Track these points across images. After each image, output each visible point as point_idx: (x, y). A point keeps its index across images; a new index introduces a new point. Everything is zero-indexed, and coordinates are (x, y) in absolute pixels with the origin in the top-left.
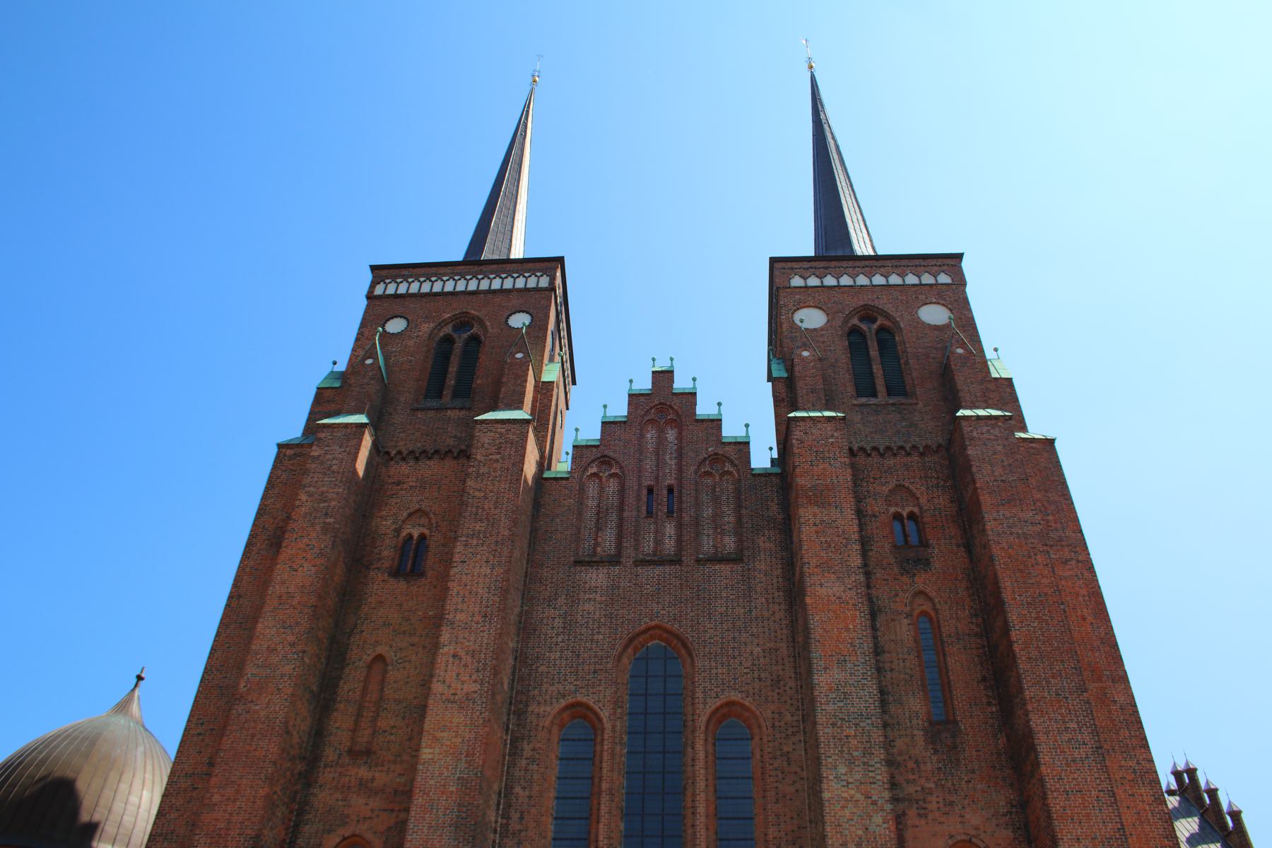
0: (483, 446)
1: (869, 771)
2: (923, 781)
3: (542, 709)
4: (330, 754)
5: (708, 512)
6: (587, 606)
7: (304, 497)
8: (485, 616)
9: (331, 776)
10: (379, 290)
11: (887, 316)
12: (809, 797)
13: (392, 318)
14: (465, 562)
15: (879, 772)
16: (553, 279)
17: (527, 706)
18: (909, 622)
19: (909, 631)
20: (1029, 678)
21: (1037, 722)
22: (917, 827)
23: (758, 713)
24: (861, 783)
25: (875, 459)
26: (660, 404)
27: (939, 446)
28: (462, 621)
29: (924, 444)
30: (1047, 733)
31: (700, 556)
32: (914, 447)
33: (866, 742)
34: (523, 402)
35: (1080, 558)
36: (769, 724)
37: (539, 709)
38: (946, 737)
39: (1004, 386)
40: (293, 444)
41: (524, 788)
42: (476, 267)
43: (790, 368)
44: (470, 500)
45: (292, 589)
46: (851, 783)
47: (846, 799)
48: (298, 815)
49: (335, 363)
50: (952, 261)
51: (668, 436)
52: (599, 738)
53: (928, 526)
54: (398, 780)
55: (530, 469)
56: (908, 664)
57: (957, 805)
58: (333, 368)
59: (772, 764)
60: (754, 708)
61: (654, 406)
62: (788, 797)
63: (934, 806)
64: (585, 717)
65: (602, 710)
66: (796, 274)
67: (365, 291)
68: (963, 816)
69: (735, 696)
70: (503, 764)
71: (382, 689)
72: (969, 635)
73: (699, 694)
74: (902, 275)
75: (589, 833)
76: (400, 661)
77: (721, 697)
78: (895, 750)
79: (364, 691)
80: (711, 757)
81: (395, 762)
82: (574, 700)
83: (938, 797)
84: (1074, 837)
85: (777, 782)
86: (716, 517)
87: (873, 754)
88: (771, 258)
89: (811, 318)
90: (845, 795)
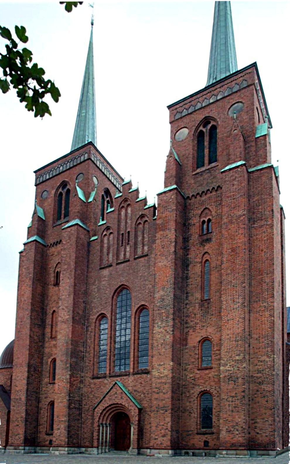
17: (89, 316)
47: (159, 332)
78: (189, 312)
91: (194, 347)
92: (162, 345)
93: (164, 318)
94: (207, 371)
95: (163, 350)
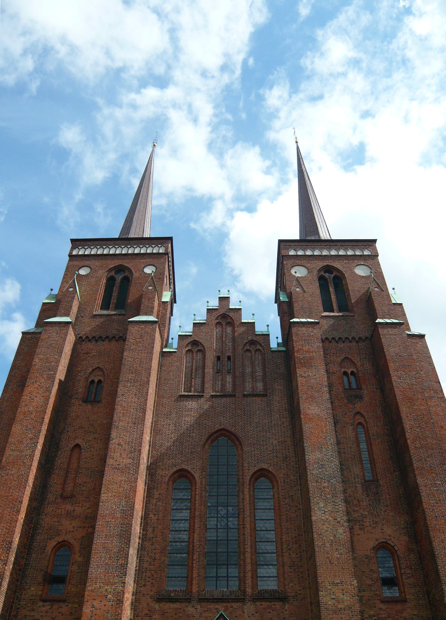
0: (133, 335)
1: (335, 506)
2: (361, 511)
3: (164, 473)
4: (51, 497)
5: (248, 370)
6: (187, 419)
7: (37, 360)
9: (51, 509)
10: (75, 253)
12: (303, 519)
14: (124, 395)
15: (340, 506)
16: (167, 249)
17: (156, 471)
18: (353, 428)
19: (353, 432)
20: (416, 458)
22: (359, 535)
23: (276, 475)
25: (334, 344)
26: (223, 314)
27: (366, 338)
28: (123, 426)
29: (358, 336)
30: (426, 486)
31: (245, 393)
32: (353, 338)
34: (153, 312)
35: (439, 396)
36: (282, 480)
37: (162, 472)
38: (373, 488)
40: (30, 332)
42: (127, 241)
44: (126, 363)
45: (31, 409)
46: (326, 512)
48: (33, 530)
49: (52, 290)
51: (227, 330)
52: (194, 488)
53: (361, 378)
54: (87, 511)
57: (379, 523)
58: (51, 292)
59: (284, 502)
60: (274, 472)
61: (220, 315)
63: (368, 524)
64: (186, 477)
65: (195, 473)
67: (68, 253)
68: (383, 529)
69: (265, 466)
73: (246, 465)
76: (89, 447)
77: (257, 466)
79: (69, 463)
80: (252, 498)
81: (86, 501)
82: (181, 468)
83: (370, 519)
84: (441, 540)
85: (287, 511)
86: (253, 372)
87: (337, 496)
89: (299, 272)
90: (323, 518)
91: (367, 557)
92: (331, 545)
94: (399, 607)
95: (336, 554)
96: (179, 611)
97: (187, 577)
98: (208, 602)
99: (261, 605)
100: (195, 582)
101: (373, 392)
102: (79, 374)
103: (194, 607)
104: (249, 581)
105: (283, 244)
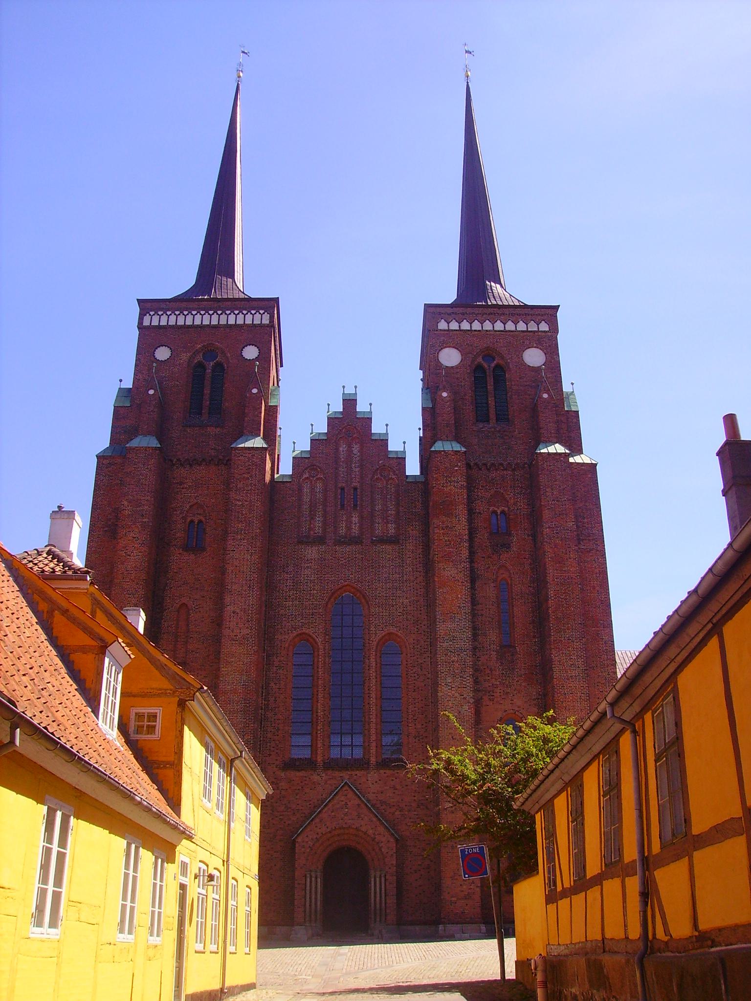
0: (238, 467)
6: (306, 572)
8: (250, 587)
10: (146, 322)
11: (503, 358)
13: (159, 347)
14: (235, 551)
21: (555, 656)
24: (459, 687)
31: (375, 539)
33: (463, 664)
36: (412, 646)
39: (573, 417)
41: (276, 684)
43: (434, 401)
49: (121, 381)
50: (549, 313)
51: (353, 449)
52: (316, 653)
55: (268, 478)
56: (491, 612)
62: (420, 689)
64: (308, 640)
66: (442, 319)
69: (393, 630)
70: (264, 671)
71: (188, 625)
72: (528, 594)
74: (516, 324)
75: (313, 708)
77: (385, 630)
88: (428, 307)
90: (449, 694)
93: (456, 671)
96: (305, 779)
97: (311, 746)
98: (333, 770)
99: (385, 773)
100: (319, 752)
101: (524, 539)
102: (175, 512)
103: (319, 775)
104: (373, 751)
105: (433, 312)
